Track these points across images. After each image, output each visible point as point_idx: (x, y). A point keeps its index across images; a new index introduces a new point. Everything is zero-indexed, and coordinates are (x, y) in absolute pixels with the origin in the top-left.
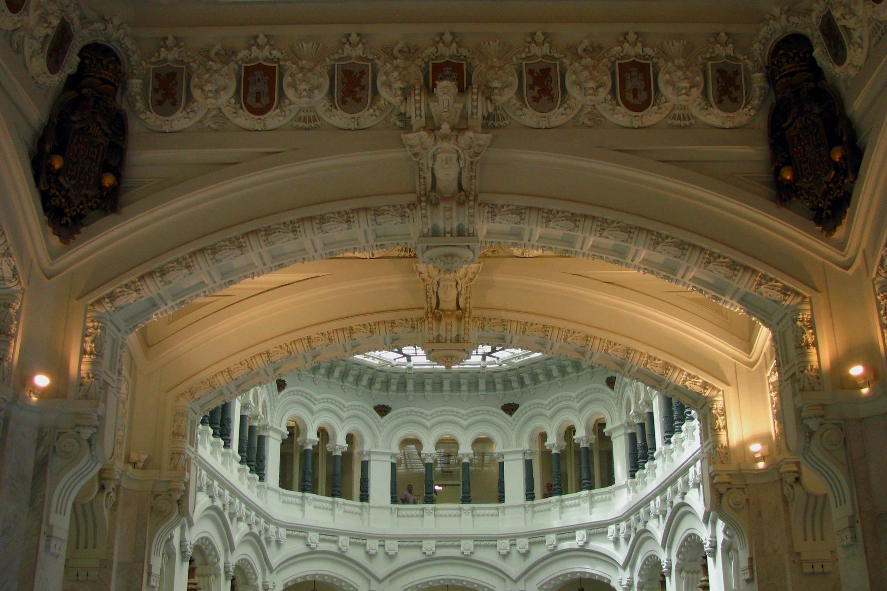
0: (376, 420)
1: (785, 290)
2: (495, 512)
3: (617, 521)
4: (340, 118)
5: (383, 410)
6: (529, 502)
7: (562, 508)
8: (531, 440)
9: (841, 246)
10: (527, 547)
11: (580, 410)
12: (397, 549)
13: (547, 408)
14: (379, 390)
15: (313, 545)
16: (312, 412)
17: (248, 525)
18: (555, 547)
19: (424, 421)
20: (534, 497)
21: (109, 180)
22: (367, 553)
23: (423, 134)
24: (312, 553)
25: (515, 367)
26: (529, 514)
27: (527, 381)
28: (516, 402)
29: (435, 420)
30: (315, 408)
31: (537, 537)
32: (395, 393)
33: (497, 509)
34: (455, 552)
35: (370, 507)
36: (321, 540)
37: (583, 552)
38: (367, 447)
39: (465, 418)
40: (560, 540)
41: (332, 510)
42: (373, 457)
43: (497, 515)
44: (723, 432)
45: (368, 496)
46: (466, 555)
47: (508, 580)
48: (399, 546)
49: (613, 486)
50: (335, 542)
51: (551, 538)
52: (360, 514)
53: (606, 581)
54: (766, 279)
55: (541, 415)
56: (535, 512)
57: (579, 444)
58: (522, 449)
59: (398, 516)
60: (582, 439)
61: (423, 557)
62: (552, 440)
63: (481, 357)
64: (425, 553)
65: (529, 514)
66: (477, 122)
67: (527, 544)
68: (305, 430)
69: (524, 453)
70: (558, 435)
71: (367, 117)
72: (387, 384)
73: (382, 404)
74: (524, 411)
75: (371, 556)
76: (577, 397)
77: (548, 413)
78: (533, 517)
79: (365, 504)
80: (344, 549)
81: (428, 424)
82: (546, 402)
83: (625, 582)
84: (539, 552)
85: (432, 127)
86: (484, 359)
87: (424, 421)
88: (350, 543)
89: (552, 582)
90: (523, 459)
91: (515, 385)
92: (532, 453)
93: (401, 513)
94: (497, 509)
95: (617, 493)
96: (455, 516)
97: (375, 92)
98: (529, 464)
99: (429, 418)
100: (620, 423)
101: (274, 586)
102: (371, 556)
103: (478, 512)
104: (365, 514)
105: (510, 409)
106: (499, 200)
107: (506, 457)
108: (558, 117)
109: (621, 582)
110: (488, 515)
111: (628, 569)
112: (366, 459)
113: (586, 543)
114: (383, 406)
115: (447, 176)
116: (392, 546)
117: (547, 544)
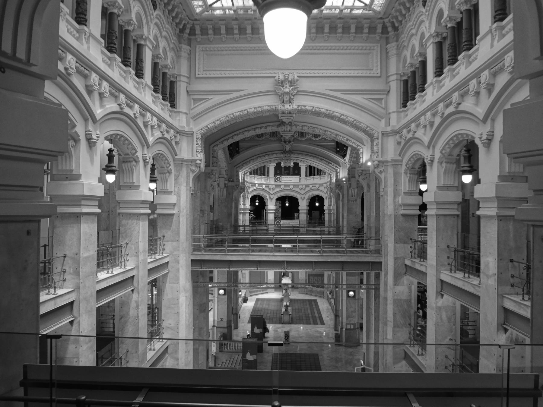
1: (336, 167)
3: (325, 183)
4: (271, 139)
9: (345, 160)
21: (237, 149)
23: (284, 143)
31: (307, 186)
34: (289, 188)
37: (317, 189)
51: (311, 186)
54: (333, 165)
66: (292, 140)
71: (276, 139)
84: (307, 189)
85: (285, 142)
97: (277, 135)
106: (294, 152)
108: (304, 139)
115: (287, 149)
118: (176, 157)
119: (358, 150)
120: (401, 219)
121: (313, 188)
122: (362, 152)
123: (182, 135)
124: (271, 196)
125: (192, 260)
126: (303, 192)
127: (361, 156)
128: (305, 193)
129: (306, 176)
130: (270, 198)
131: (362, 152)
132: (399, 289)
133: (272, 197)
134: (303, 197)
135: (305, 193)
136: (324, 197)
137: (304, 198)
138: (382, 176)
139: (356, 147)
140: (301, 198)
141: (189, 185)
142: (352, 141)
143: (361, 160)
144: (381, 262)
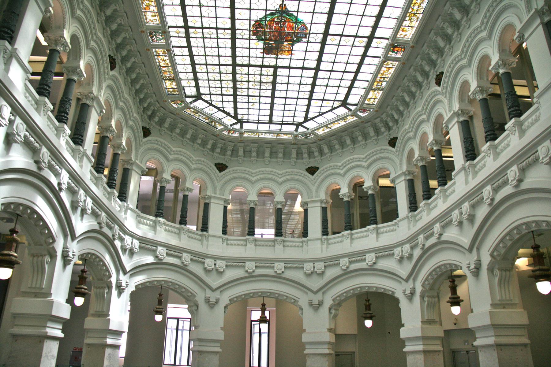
0: (216, 175)
2: (301, 244)
3: (401, 244)
5: (221, 167)
6: (325, 237)
7: (352, 239)
8: (326, 194)
10: (323, 268)
11: (368, 167)
12: (225, 267)
13: (341, 168)
14: (220, 154)
15: (161, 257)
16: (168, 160)
17: (98, 223)
18: (347, 267)
19: (250, 177)
20: (328, 233)
22: (205, 269)
24: (159, 264)
25: (320, 138)
26: (325, 246)
27: (326, 150)
28: (317, 165)
32: (230, 157)
33: (302, 242)
34: (270, 272)
35: (209, 236)
36: (167, 254)
37: (372, 270)
38: (209, 193)
39: (280, 176)
40: (351, 262)
41: (179, 234)
42: (213, 200)
43: (302, 247)
45: (207, 228)
46: (278, 274)
47: (309, 292)
48: (226, 266)
49: (398, 219)
50: (180, 258)
51: (344, 262)
52: (200, 240)
53: (390, 293)
56: (328, 244)
57: (367, 192)
58: (320, 199)
59: (228, 244)
60: (370, 187)
61: (246, 275)
62: (345, 190)
63: (295, 127)
64: (247, 271)
65: (325, 246)
67: (323, 267)
68: (163, 171)
69: (322, 201)
70: (349, 187)
72: (223, 151)
73: (221, 163)
74: (322, 172)
75: (207, 271)
76: (366, 157)
77: (342, 172)
78: (327, 248)
79: (205, 233)
80: (186, 263)
81: (253, 179)
83: (408, 292)
86: (297, 130)
87: (250, 177)
88: (191, 260)
89: (352, 291)
90: (321, 206)
91: (316, 154)
92: (327, 202)
93: (229, 242)
94: (302, 242)
95: (400, 224)
96: (270, 246)
98: (324, 210)
99: (253, 175)
100: (401, 172)
101: (127, 285)
102: (207, 271)
103: (288, 244)
104: (205, 242)
105: (312, 171)
107: (309, 205)
109: (405, 292)
110: (295, 246)
111: (411, 281)
112: (207, 202)
113: (374, 263)
114: (222, 164)
116: (221, 264)
117: (341, 265)
121: (354, 267)
124: (209, 293)
126: (315, 283)
128: (324, 289)
129: (325, 232)
130: (207, 301)
133: (213, 300)
134: (316, 299)
135: (324, 289)
136: (399, 294)
137: (320, 304)
140: (311, 304)
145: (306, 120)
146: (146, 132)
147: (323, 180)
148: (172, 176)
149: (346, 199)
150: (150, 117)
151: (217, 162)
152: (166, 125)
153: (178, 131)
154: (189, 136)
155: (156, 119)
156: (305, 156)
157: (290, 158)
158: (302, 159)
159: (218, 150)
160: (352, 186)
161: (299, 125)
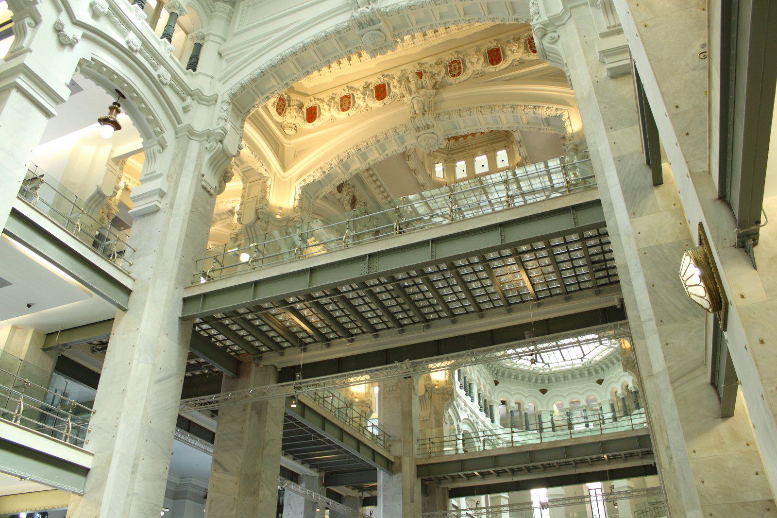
5: (544, 391)
8: (611, 395)
29: (567, 393)
30: (513, 393)
44: (623, 344)
55: (614, 382)
62: (619, 392)
69: (609, 400)
70: (622, 388)
77: (616, 380)
82: (613, 376)
92: (612, 400)
105: (600, 382)
118: (178, 126)
119: (560, 116)
120: (612, 84)
122: (569, 118)
123: (199, 103)
125: (185, 300)
127: (567, 123)
131: (569, 118)
132: (645, 222)
138: (559, 47)
139: (553, 113)
141: (201, 169)
142: (543, 107)
143: (569, 130)
144: (597, 203)
145: (584, 355)
146: (496, 383)
147: (608, 387)
148: (516, 403)
149: (621, 397)
150: (496, 374)
151: (540, 389)
152: (506, 375)
153: (513, 377)
154: (520, 378)
155: (500, 374)
156: (594, 373)
157: (585, 377)
158: (593, 375)
159: (540, 381)
160: (624, 388)
161: (582, 358)
